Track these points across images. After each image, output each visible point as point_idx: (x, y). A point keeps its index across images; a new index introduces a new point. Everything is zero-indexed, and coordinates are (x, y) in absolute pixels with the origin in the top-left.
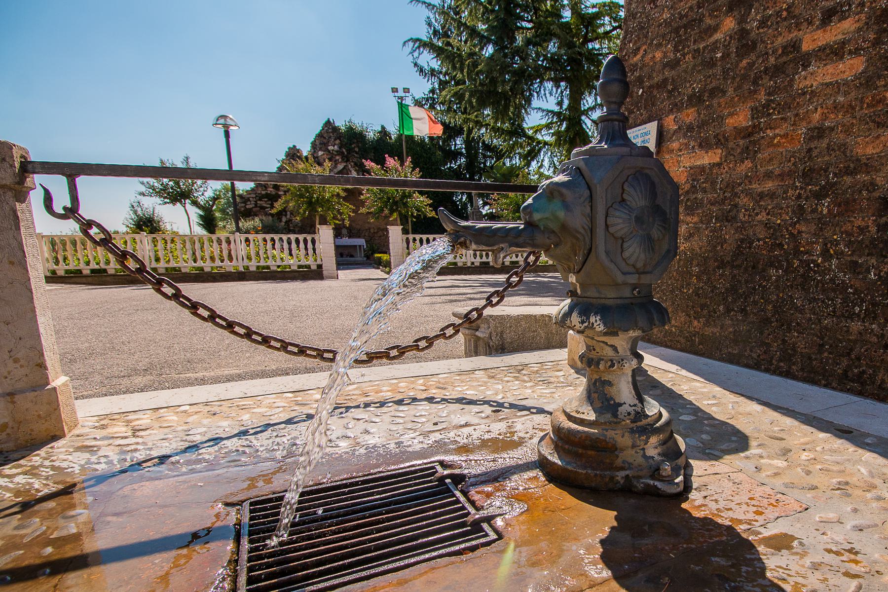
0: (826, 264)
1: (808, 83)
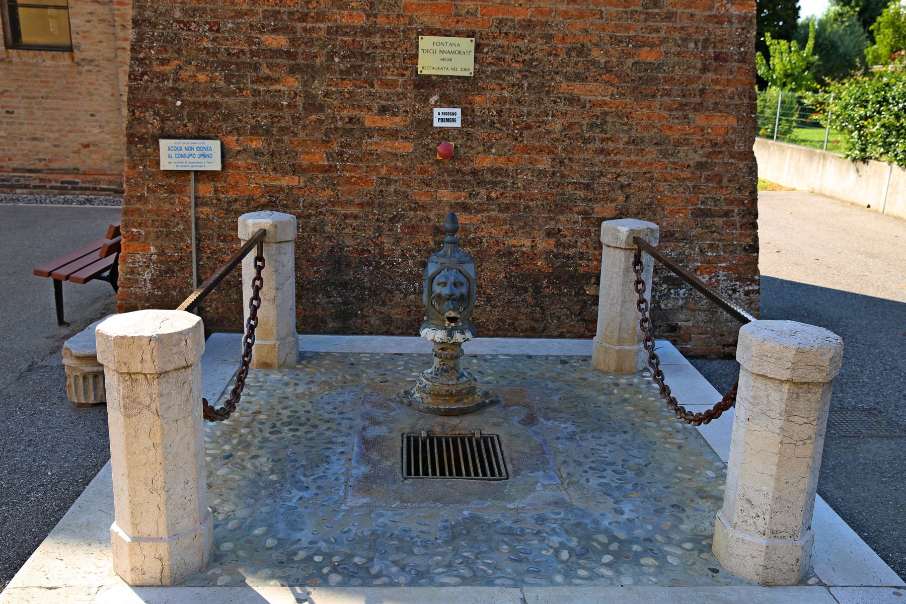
1: (373, 147)
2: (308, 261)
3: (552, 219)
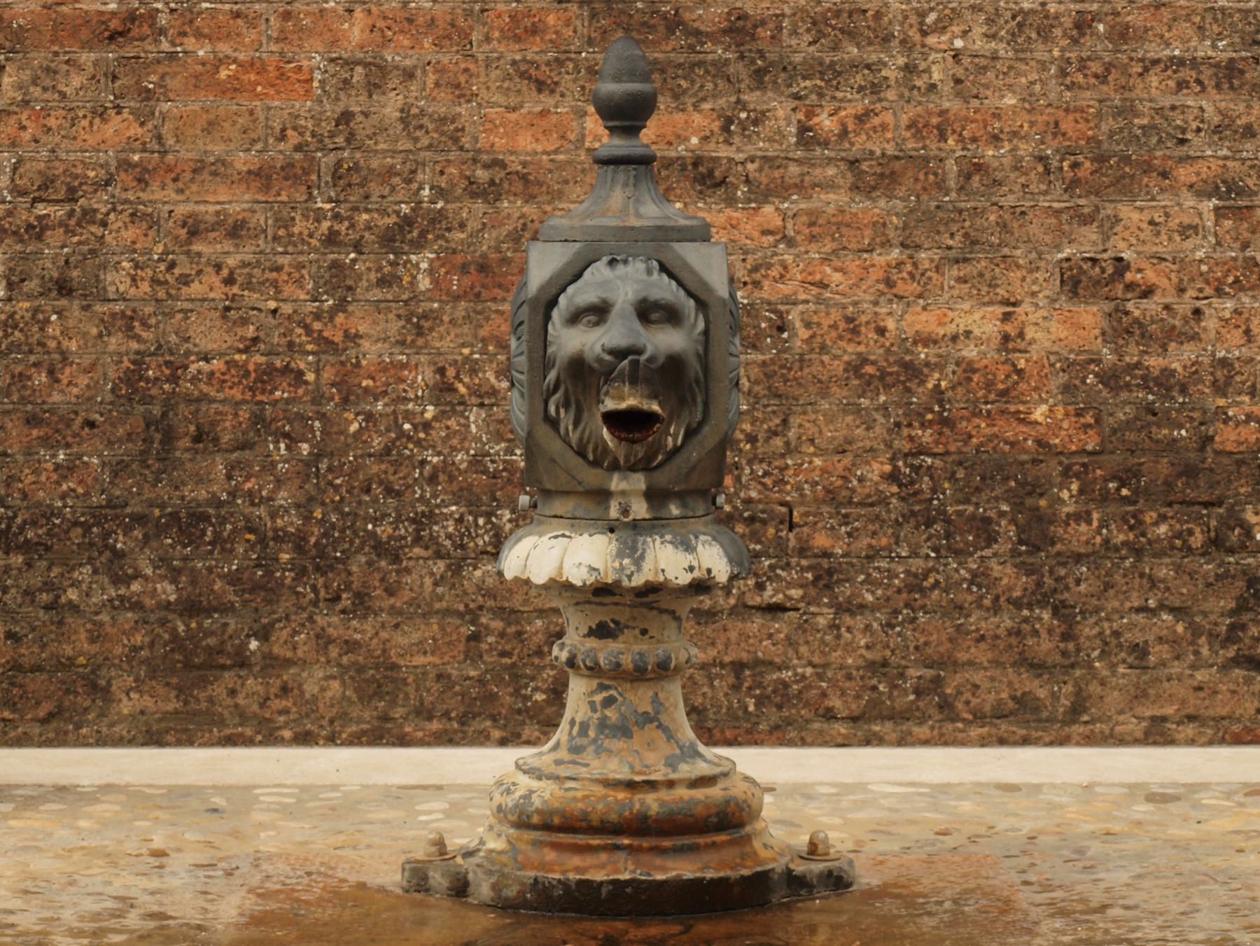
0: (452, 422)
2: (32, 421)
3: (1086, 220)
